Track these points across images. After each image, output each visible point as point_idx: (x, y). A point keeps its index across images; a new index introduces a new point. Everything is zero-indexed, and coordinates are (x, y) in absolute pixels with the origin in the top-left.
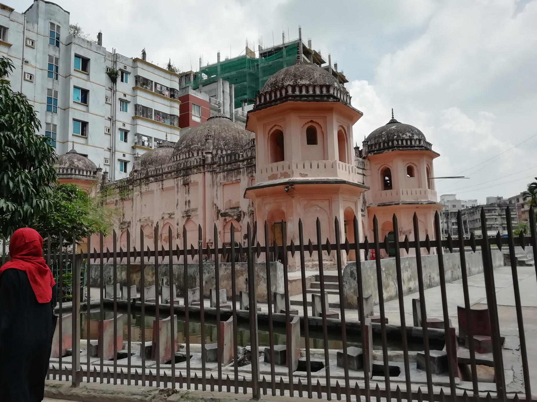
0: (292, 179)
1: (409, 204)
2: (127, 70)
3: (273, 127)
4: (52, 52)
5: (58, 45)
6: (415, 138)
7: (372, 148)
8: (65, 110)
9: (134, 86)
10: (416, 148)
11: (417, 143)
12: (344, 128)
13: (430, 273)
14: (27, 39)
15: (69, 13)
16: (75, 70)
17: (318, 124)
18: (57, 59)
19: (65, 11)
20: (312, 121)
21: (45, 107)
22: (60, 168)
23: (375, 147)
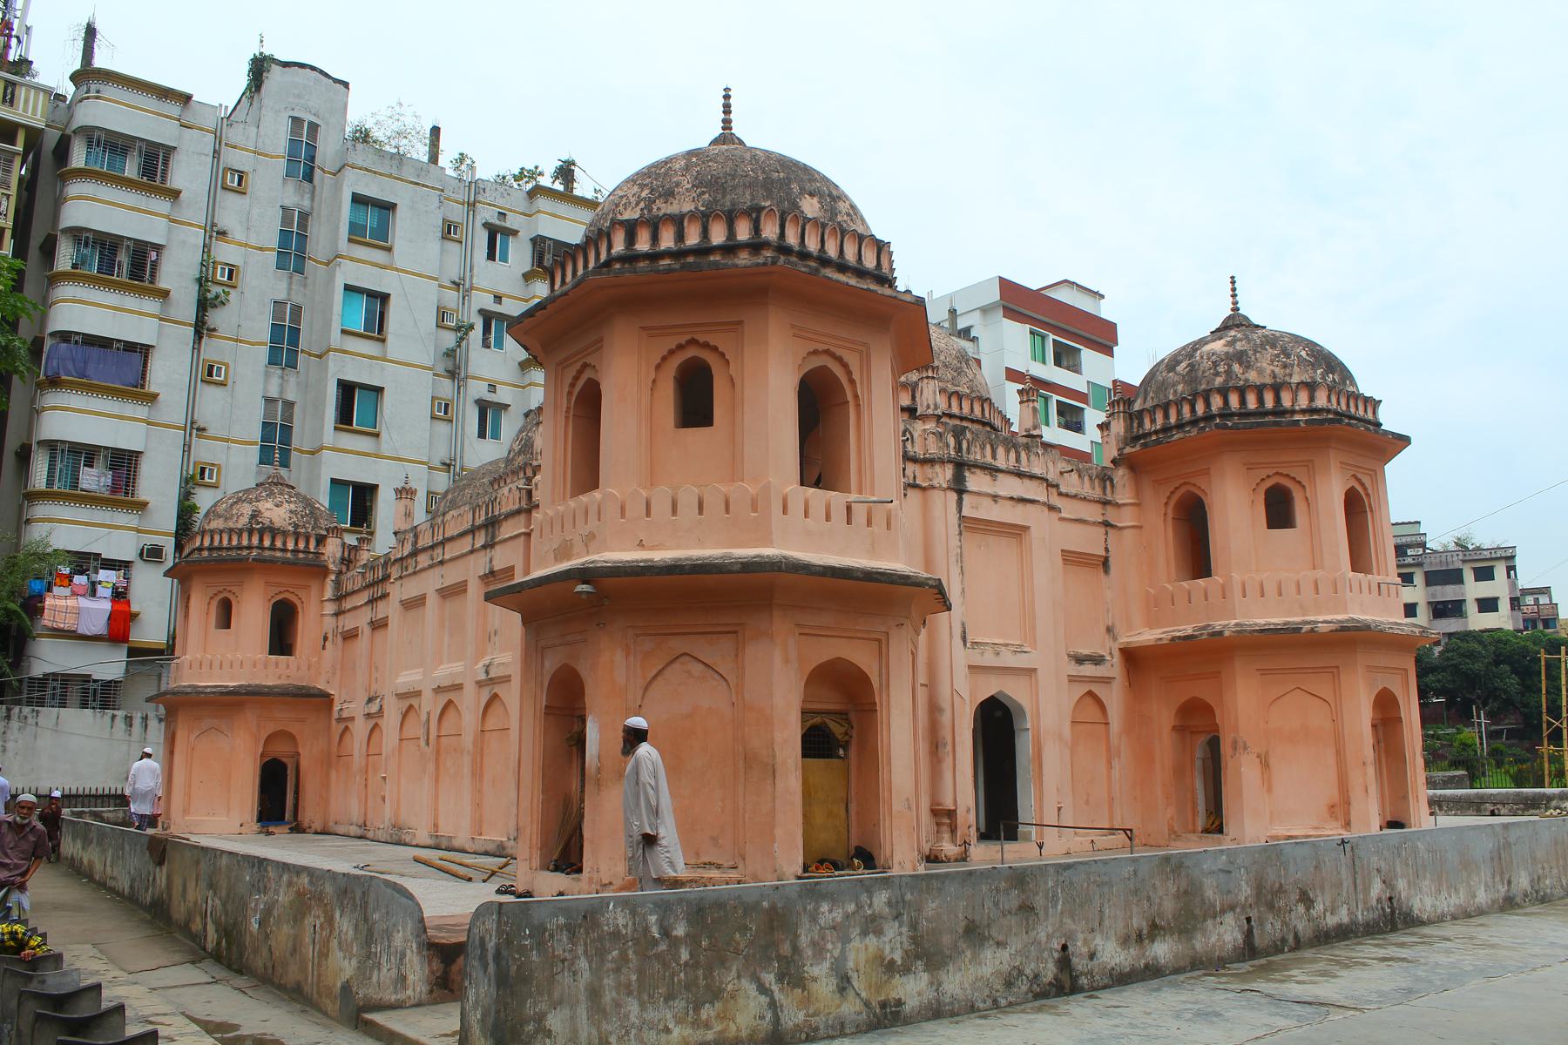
0: (595, 557)
1: (1262, 631)
2: (508, 224)
3: (580, 372)
4: (291, 196)
5: (309, 177)
6: (1295, 379)
7: (1141, 424)
8: (320, 357)
9: (528, 268)
10: (1296, 417)
11: (1303, 401)
12: (840, 360)
13: (1070, 936)
14: (226, 170)
15: (346, 85)
16: (350, 240)
17: (715, 349)
18: (304, 217)
19: (336, 81)
20: (693, 342)
21: (263, 353)
22: (221, 532)
23: (1153, 421)
